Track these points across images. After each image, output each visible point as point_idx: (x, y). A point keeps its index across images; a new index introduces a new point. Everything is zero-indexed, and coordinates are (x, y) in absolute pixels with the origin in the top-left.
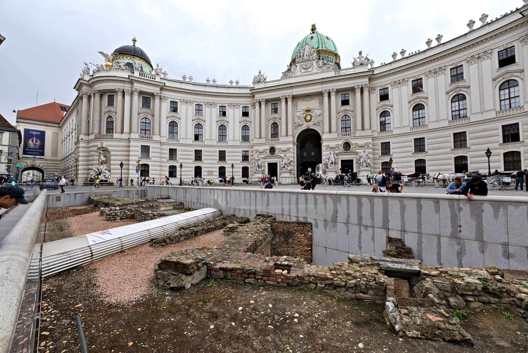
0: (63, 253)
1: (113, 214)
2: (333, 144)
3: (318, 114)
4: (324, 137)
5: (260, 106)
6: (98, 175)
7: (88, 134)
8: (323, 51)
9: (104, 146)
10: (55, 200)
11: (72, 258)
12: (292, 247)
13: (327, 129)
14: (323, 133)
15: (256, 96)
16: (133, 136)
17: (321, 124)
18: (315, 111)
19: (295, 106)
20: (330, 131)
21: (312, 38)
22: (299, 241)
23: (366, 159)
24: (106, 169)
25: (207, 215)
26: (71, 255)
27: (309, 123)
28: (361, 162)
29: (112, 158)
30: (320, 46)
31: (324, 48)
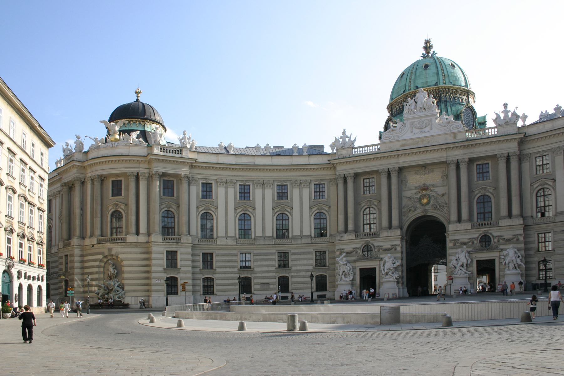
2: (464, 238)
3: (441, 193)
4: (451, 228)
5: (345, 182)
7: (83, 237)
8: (445, 88)
9: (113, 253)
13: (454, 217)
14: (449, 223)
15: (338, 168)
16: (153, 238)
17: (446, 208)
18: (436, 189)
19: (402, 182)
20: (459, 220)
21: (426, 66)
23: (514, 258)
27: (427, 207)
28: (507, 262)
29: (125, 269)
30: (441, 80)
31: (448, 85)
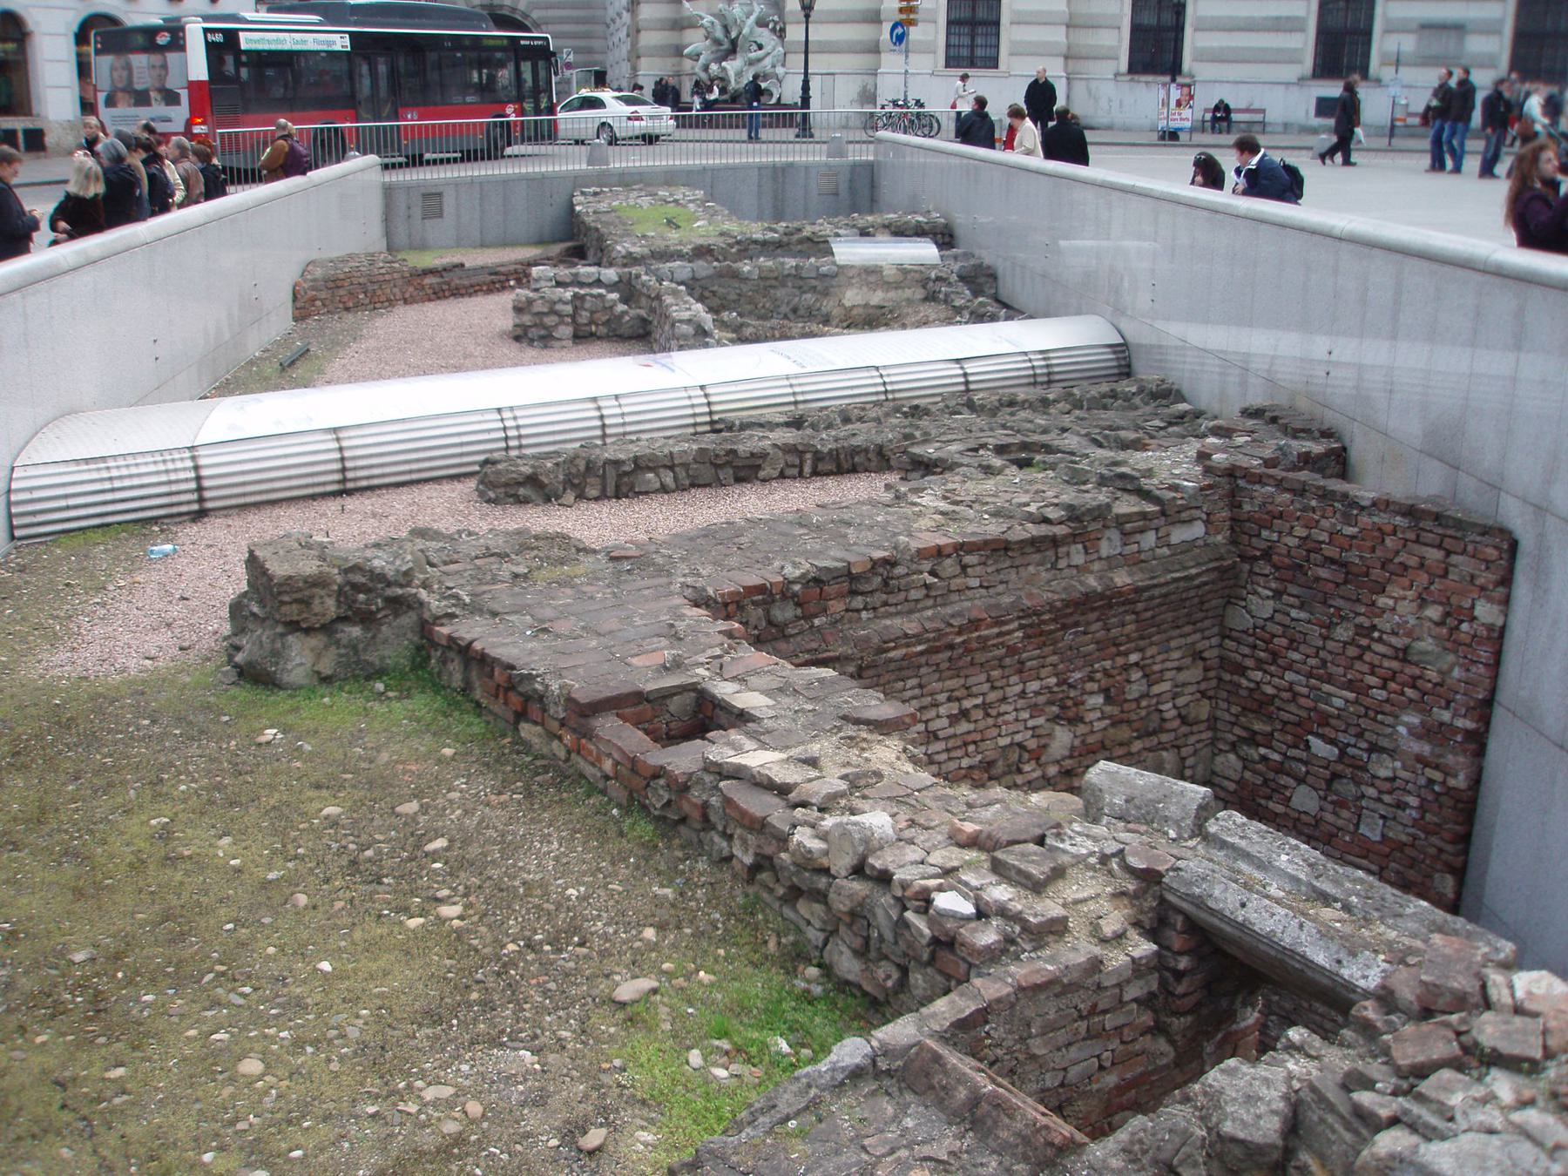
0: (87, 461)
1: (539, 307)
6: (725, 58)
10: (417, 212)
11: (117, 484)
12: (1350, 685)
22: (1403, 655)
24: (761, 23)
25: (970, 368)
26: (115, 473)
